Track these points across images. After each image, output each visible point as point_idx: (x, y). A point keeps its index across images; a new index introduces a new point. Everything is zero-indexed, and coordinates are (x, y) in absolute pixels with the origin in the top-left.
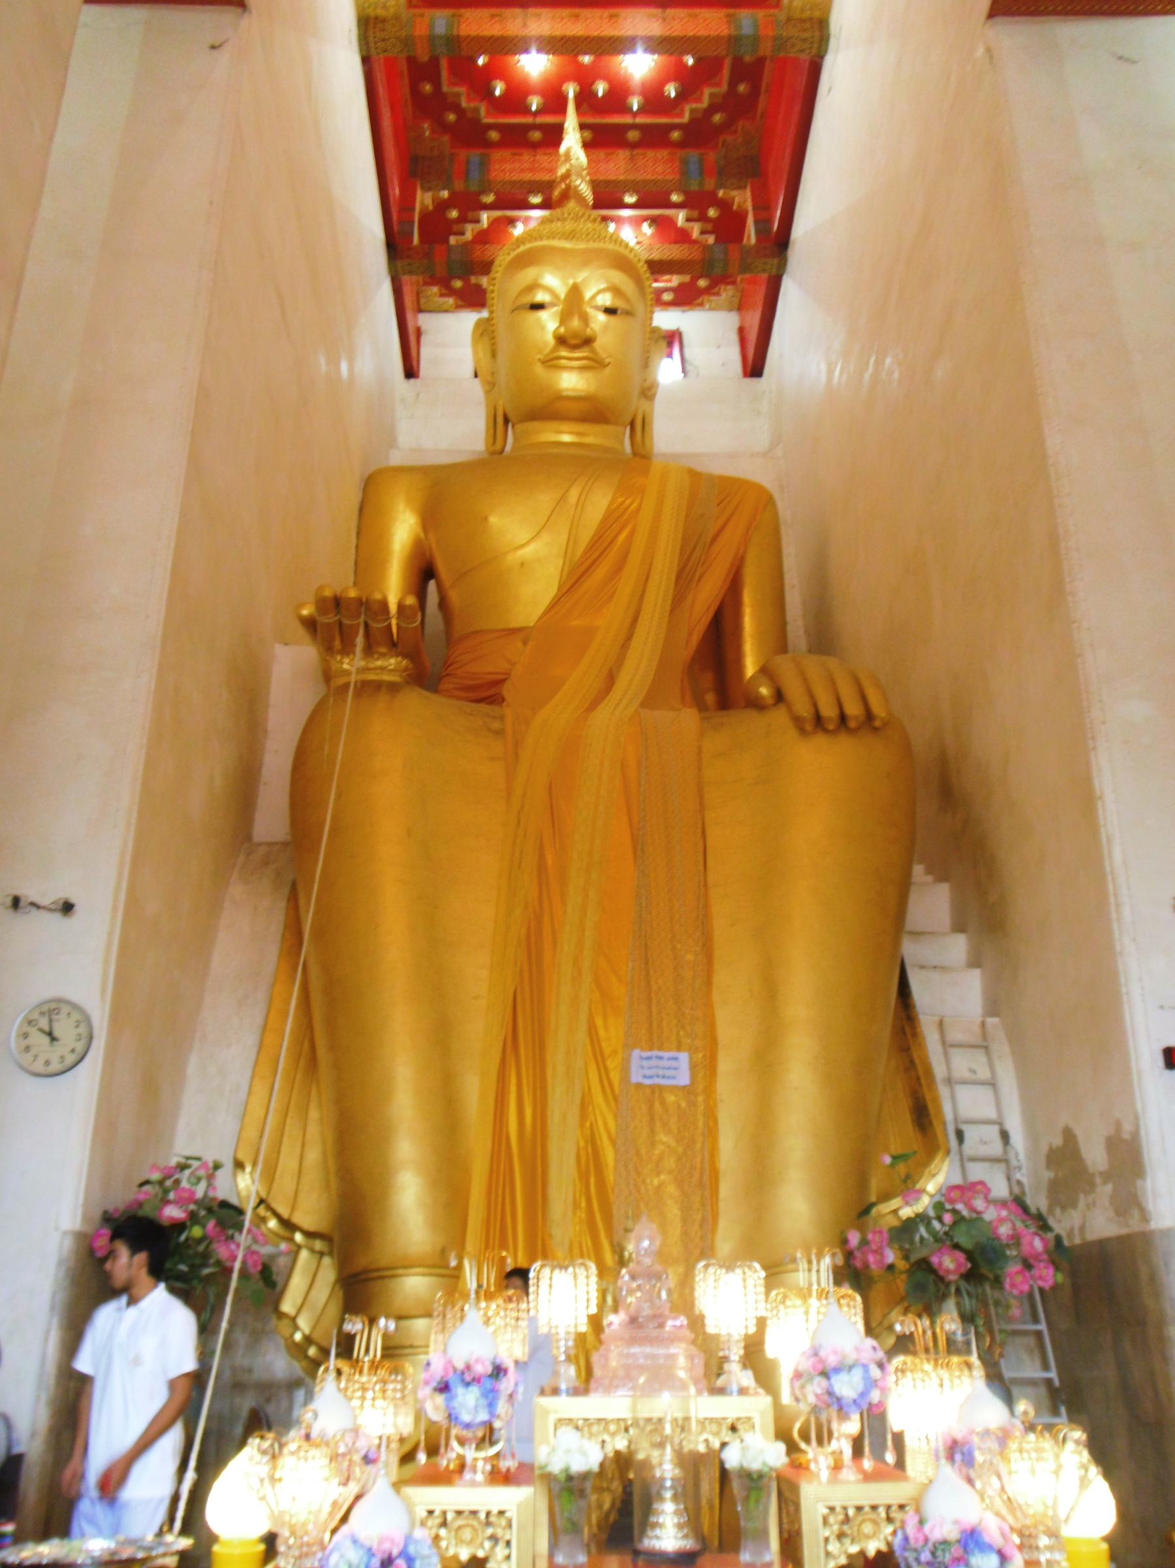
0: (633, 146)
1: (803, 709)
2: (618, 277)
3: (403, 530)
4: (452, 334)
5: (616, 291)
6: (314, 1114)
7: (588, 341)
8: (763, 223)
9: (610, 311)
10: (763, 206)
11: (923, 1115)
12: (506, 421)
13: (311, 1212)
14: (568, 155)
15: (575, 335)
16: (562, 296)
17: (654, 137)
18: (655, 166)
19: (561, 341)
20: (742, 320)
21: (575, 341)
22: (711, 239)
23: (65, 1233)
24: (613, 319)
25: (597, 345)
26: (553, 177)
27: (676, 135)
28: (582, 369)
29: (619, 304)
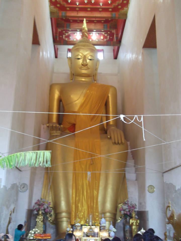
1: (113, 141)
2: (91, 54)
3: (57, 95)
4: (63, 49)
5: (91, 56)
7: (87, 65)
8: (117, 37)
9: (90, 60)
10: (117, 34)
12: (73, 74)
14: (84, 28)
15: (85, 65)
16: (83, 57)
17: (99, 22)
18: (99, 26)
19: (82, 65)
21: (85, 65)
22: (108, 37)
23: (26, 209)
24: (90, 61)
25: (88, 66)
26: (81, 28)
27: (103, 22)
28: (86, 70)
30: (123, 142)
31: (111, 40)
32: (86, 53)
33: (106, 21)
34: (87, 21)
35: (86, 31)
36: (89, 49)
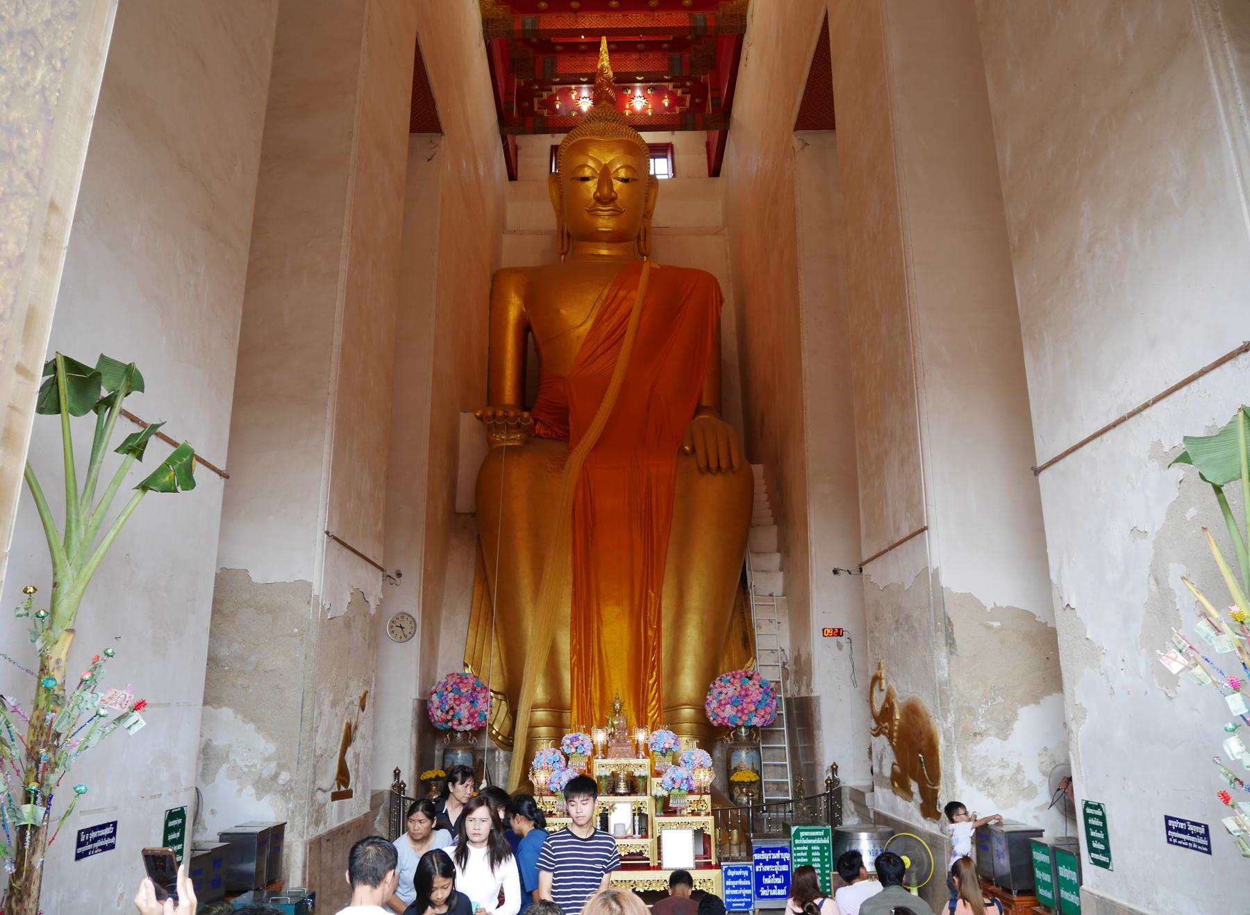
0: (640, 51)
1: (702, 463)
2: (629, 160)
3: (514, 309)
5: (627, 167)
6: (494, 643)
9: (625, 180)
11: (748, 642)
12: (569, 236)
13: (496, 683)
17: (652, 47)
18: (653, 63)
19: (598, 200)
20: (709, 137)
21: (605, 199)
22: (688, 97)
29: (629, 175)
30: (735, 463)
31: (698, 108)
32: (607, 159)
33: (679, 43)
34: (612, 46)
35: (608, 79)
36: (619, 142)
